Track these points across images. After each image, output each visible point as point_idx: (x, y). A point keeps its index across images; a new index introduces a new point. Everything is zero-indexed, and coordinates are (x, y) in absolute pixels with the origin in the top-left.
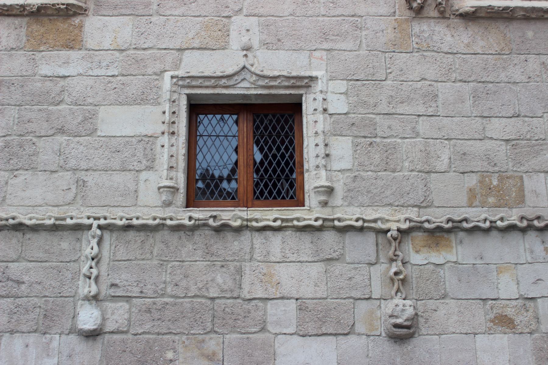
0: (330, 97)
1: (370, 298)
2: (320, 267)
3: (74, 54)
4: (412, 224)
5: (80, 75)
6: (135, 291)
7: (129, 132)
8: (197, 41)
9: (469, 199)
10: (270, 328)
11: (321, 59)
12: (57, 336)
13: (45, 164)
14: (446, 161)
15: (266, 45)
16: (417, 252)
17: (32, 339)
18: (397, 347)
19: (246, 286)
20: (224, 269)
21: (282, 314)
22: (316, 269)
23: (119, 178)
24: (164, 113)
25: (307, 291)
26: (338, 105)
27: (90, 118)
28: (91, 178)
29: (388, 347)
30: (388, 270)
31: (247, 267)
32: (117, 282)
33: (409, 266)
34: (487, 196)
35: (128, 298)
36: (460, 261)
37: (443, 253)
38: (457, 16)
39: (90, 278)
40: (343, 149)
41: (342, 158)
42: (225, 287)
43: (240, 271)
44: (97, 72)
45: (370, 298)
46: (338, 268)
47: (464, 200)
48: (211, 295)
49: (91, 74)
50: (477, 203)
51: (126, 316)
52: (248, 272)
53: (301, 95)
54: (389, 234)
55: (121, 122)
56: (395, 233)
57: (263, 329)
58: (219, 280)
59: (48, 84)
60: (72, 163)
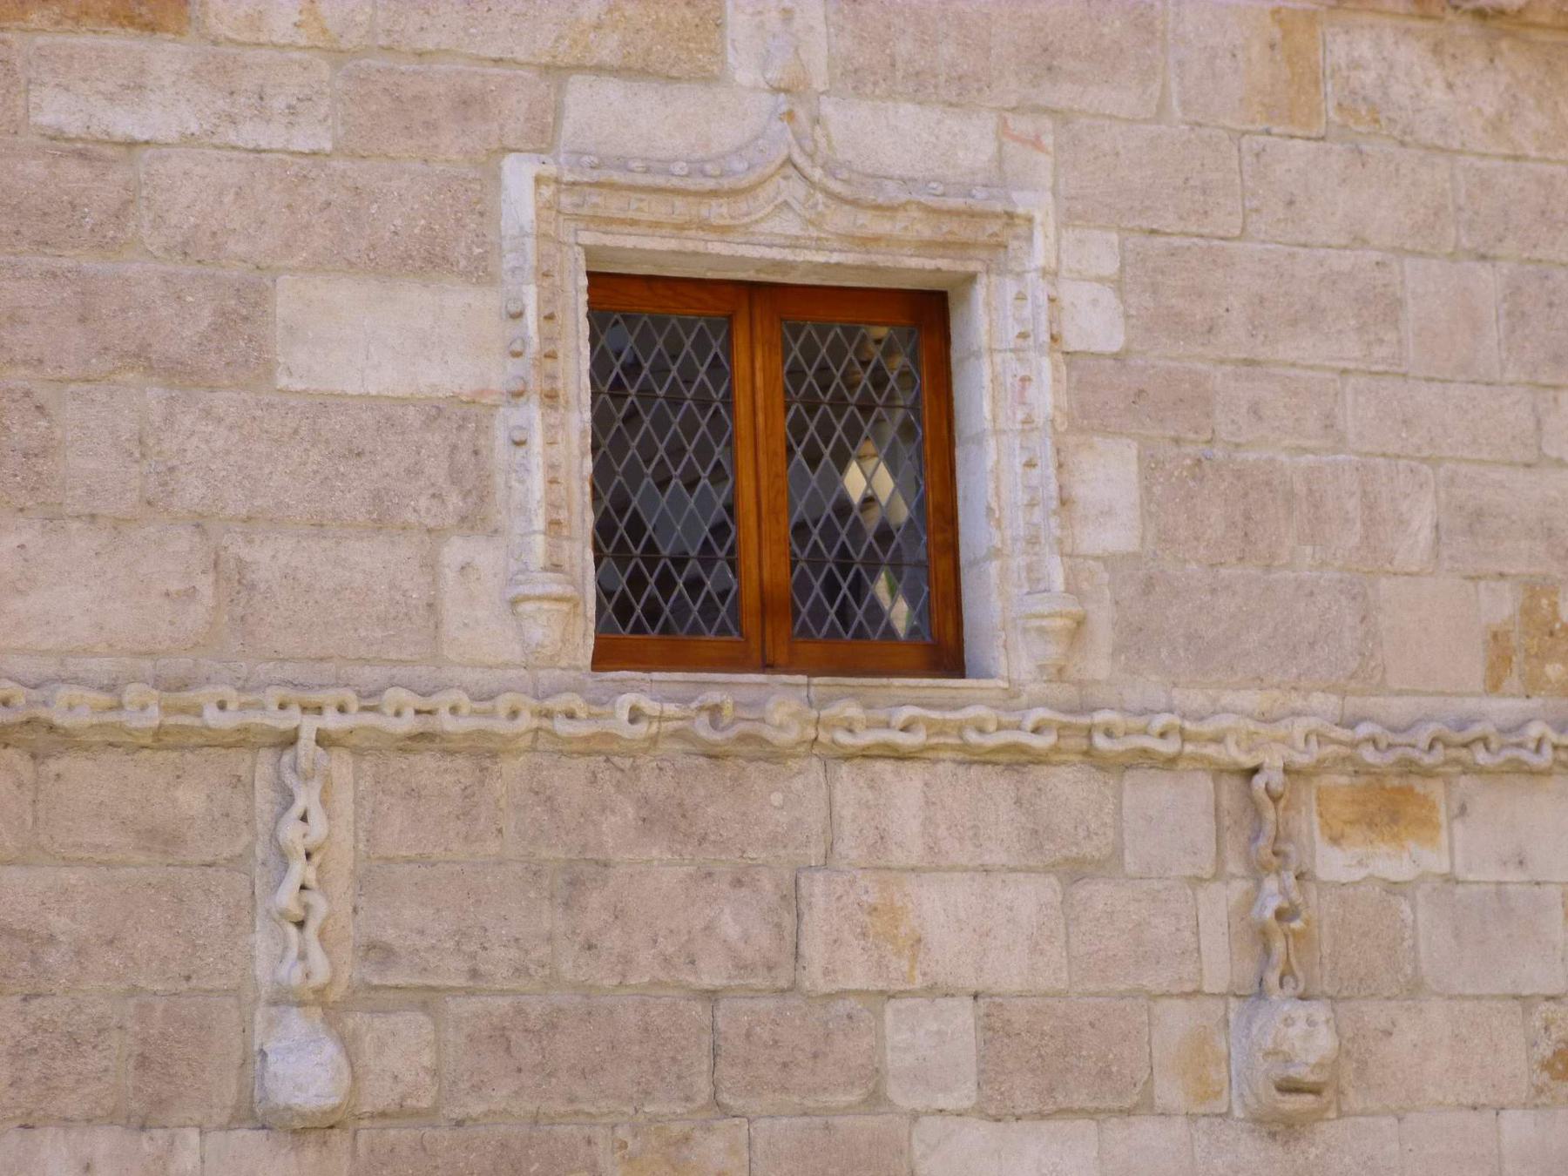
0: (1068, 291)
1: (1197, 992)
2: (1046, 888)
3: (165, 56)
4: (1330, 749)
5: (188, 140)
6: (452, 973)
7: (385, 379)
8: (613, 40)
9: (1492, 667)
10: (894, 1091)
11: (1037, 144)
12: (193, 1136)
13: (91, 492)
14: (1425, 535)
15: (854, 80)
16: (1335, 840)
17: (102, 1143)
18: (1277, 1151)
19: (815, 951)
20: (744, 892)
21: (929, 1045)
22: (1031, 896)
23: (370, 559)
24: (518, 316)
25: (1010, 972)
26: (1098, 324)
27: (242, 317)
28: (268, 557)
29: (1250, 1149)
30: (1252, 898)
31: (817, 889)
32: (389, 935)
33: (1312, 890)
34: (1543, 657)
35: (427, 999)
36: (1461, 873)
37: (1411, 845)
38: (1465, 12)
39: (300, 924)
40: (1111, 475)
41: (1108, 512)
42: (749, 954)
43: (793, 899)
44: (250, 133)
45: (1197, 992)
46: (1099, 894)
47: (1474, 670)
48: (707, 982)
49: (232, 137)
50: (1513, 682)
51: (427, 1059)
52: (820, 902)
53: (971, 278)
54: (1259, 782)
55: (368, 344)
56: (1277, 780)
57: (875, 1100)
58: (729, 928)
59: (75, 172)
60: (192, 491)
